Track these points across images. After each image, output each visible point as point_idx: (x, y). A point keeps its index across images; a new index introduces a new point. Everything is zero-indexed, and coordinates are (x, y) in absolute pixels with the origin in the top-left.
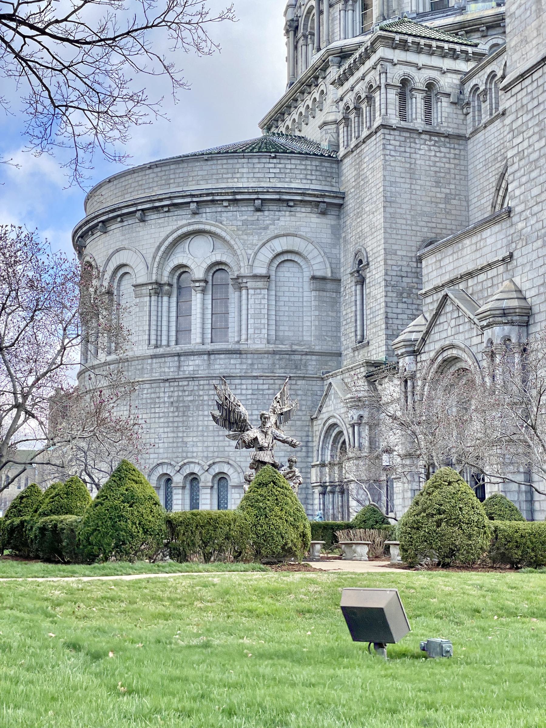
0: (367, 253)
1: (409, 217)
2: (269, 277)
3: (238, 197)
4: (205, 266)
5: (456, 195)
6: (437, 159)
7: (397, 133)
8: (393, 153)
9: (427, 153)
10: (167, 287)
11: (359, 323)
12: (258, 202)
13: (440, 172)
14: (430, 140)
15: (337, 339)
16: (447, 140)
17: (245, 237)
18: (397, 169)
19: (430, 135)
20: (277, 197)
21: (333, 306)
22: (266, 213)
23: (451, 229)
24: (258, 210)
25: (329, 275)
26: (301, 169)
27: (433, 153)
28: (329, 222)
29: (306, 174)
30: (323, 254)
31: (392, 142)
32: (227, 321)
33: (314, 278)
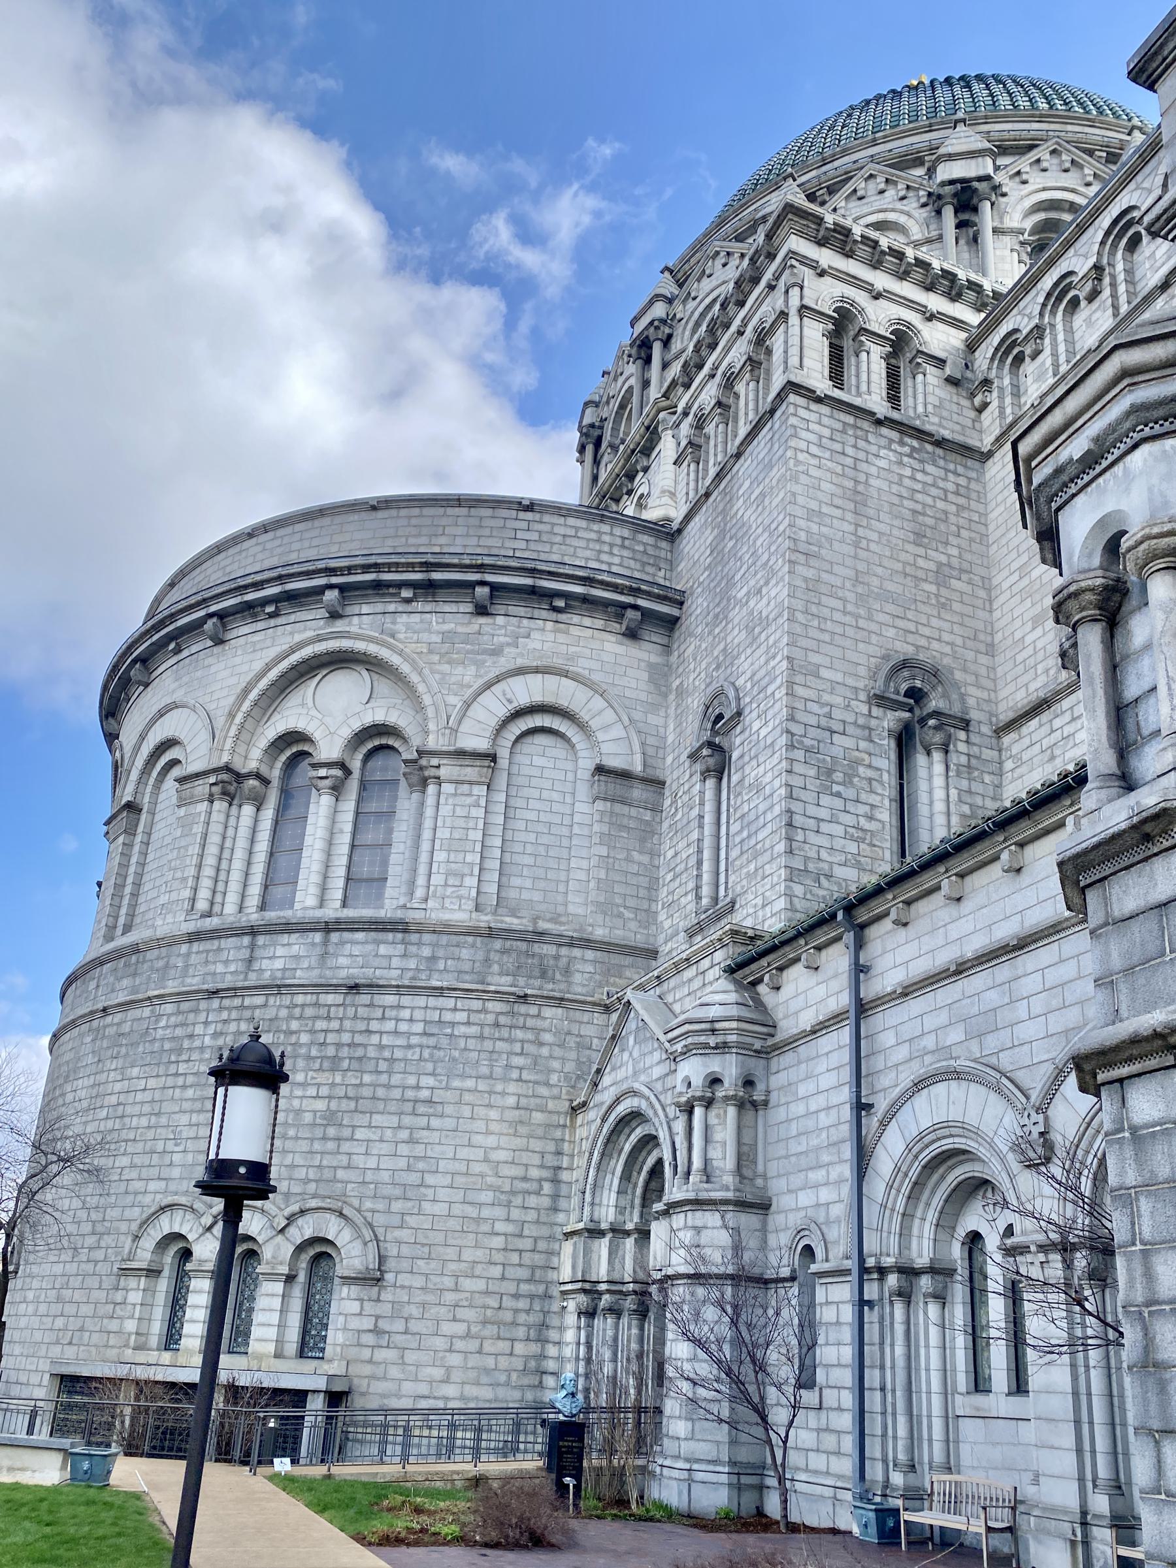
0: (737, 690)
1: (851, 596)
2: (493, 758)
3: (436, 576)
4: (346, 733)
5: (961, 571)
6: (919, 487)
7: (825, 410)
8: (814, 449)
9: (895, 468)
10: (253, 782)
11: (706, 866)
12: (482, 592)
13: (924, 514)
14: (902, 443)
15: (648, 917)
16: (939, 451)
17: (446, 668)
18: (826, 486)
19: (901, 432)
20: (528, 581)
21: (643, 840)
22: (500, 620)
23: (952, 644)
24: (482, 610)
25: (638, 768)
26: (588, 540)
27: (908, 472)
28: (644, 656)
29: (600, 552)
30: (627, 722)
31: (812, 426)
32: (385, 863)
33: (600, 770)
